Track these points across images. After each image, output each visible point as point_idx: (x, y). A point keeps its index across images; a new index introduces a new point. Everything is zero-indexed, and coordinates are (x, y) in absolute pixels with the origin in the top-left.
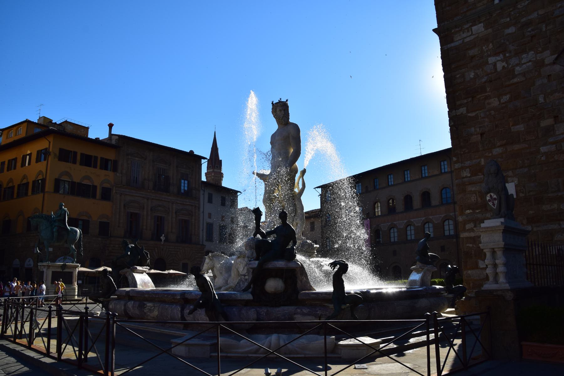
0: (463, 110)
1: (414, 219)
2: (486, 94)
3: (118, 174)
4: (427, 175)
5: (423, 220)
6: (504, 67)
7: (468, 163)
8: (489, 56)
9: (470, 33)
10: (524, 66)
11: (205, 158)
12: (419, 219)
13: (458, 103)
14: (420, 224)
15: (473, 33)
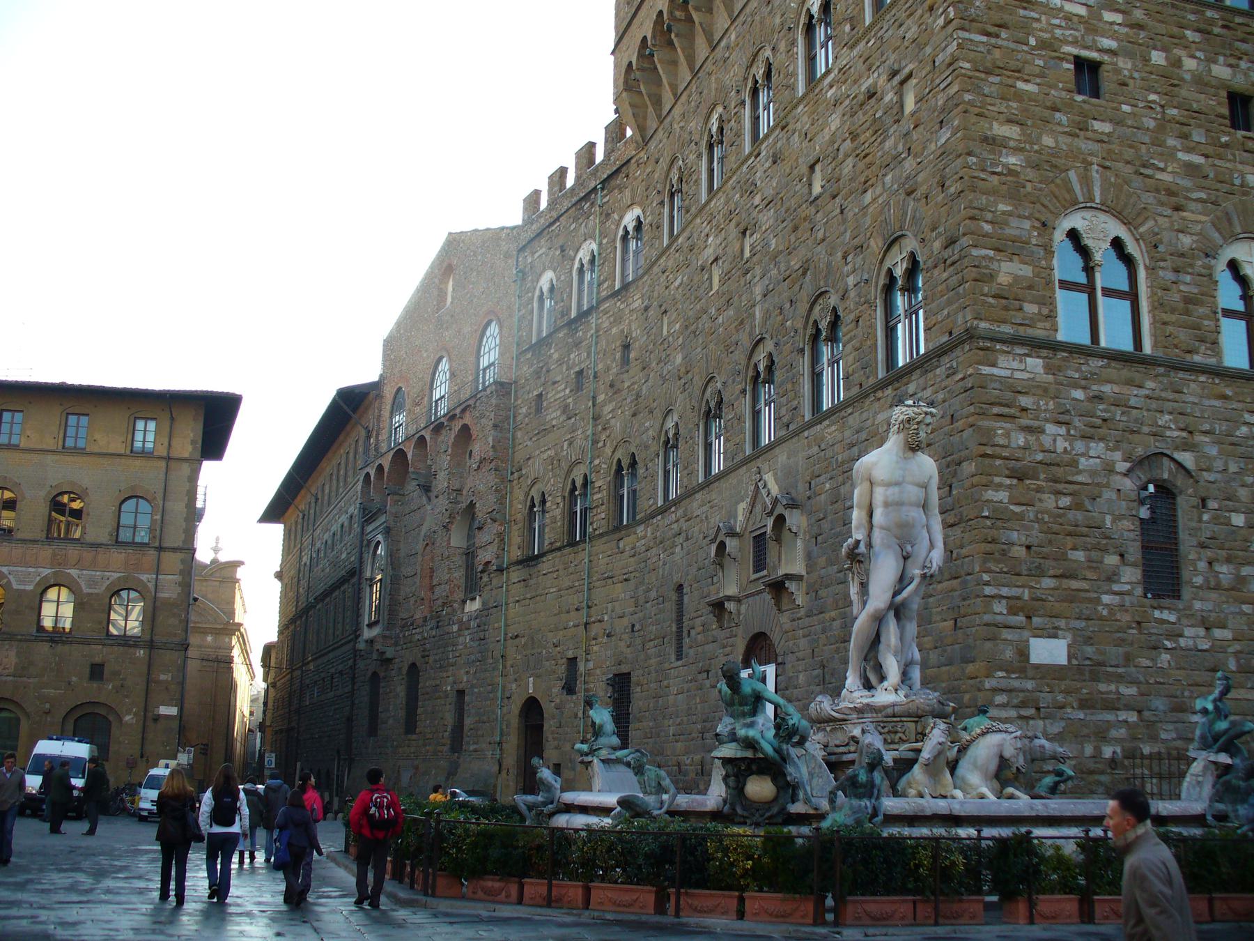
0: (1003, 496)
2: (1039, 483)
4: (81, 444)
6: (1065, 448)
7: (1005, 591)
8: (1047, 420)
10: (1091, 460)
12: (30, 569)
13: (997, 480)
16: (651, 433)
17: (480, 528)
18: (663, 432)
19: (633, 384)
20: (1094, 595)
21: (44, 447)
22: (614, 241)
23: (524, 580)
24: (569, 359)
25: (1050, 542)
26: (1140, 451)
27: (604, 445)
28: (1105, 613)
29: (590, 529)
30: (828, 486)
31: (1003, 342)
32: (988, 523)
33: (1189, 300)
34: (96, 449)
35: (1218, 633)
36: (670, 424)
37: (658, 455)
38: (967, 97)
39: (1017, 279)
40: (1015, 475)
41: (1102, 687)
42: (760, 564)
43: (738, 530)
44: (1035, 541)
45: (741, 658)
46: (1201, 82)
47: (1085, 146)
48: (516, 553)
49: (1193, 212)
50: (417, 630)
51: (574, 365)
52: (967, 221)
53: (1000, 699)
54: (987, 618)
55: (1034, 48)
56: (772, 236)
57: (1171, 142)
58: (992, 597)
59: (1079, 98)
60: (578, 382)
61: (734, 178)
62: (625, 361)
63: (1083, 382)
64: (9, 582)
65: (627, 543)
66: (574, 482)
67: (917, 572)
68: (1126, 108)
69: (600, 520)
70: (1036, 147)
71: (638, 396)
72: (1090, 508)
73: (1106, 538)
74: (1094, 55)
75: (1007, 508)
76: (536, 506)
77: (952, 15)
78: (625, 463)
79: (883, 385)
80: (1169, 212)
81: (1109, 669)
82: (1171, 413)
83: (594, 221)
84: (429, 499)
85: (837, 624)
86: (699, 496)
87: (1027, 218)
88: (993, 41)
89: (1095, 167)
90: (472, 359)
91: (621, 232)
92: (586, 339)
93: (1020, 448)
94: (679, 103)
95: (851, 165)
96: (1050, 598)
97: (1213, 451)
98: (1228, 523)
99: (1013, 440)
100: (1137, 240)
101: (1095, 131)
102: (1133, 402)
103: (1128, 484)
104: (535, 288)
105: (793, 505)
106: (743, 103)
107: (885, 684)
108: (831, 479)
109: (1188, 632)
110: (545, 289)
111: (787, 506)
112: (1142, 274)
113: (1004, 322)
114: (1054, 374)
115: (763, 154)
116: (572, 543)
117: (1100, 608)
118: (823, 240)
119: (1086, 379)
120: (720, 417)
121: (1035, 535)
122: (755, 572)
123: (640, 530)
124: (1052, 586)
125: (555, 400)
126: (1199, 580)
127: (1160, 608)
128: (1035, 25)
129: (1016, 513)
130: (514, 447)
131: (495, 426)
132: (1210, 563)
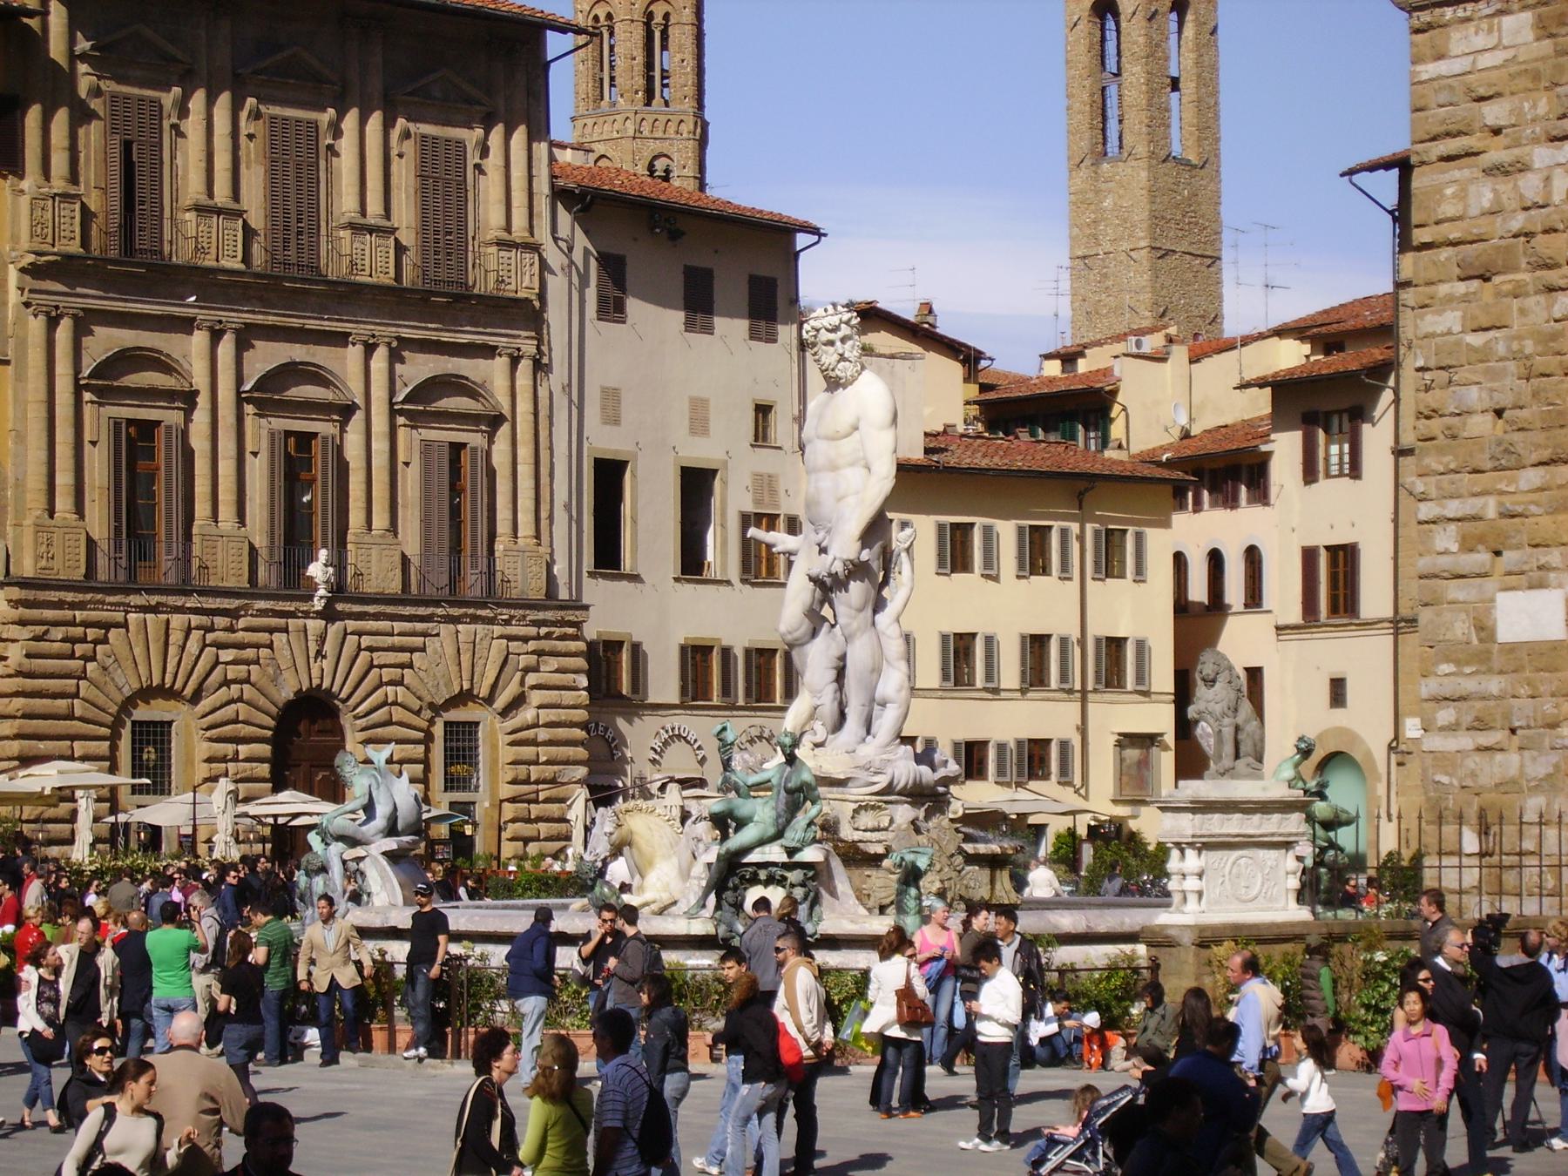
0: (1451, 320)
3: (25, 185)
7: (1453, 508)
8: (1535, 141)
11: (564, 28)
13: (1443, 289)
15: (1505, 42)
25: (1535, 394)
40: (1472, 273)
44: (1505, 400)
53: (1445, 715)
75: (1458, 343)
96: (1533, 509)
99: (1472, 201)
114: (1552, 36)
121: (1510, 387)
124: (1537, 482)
129: (1470, 347)
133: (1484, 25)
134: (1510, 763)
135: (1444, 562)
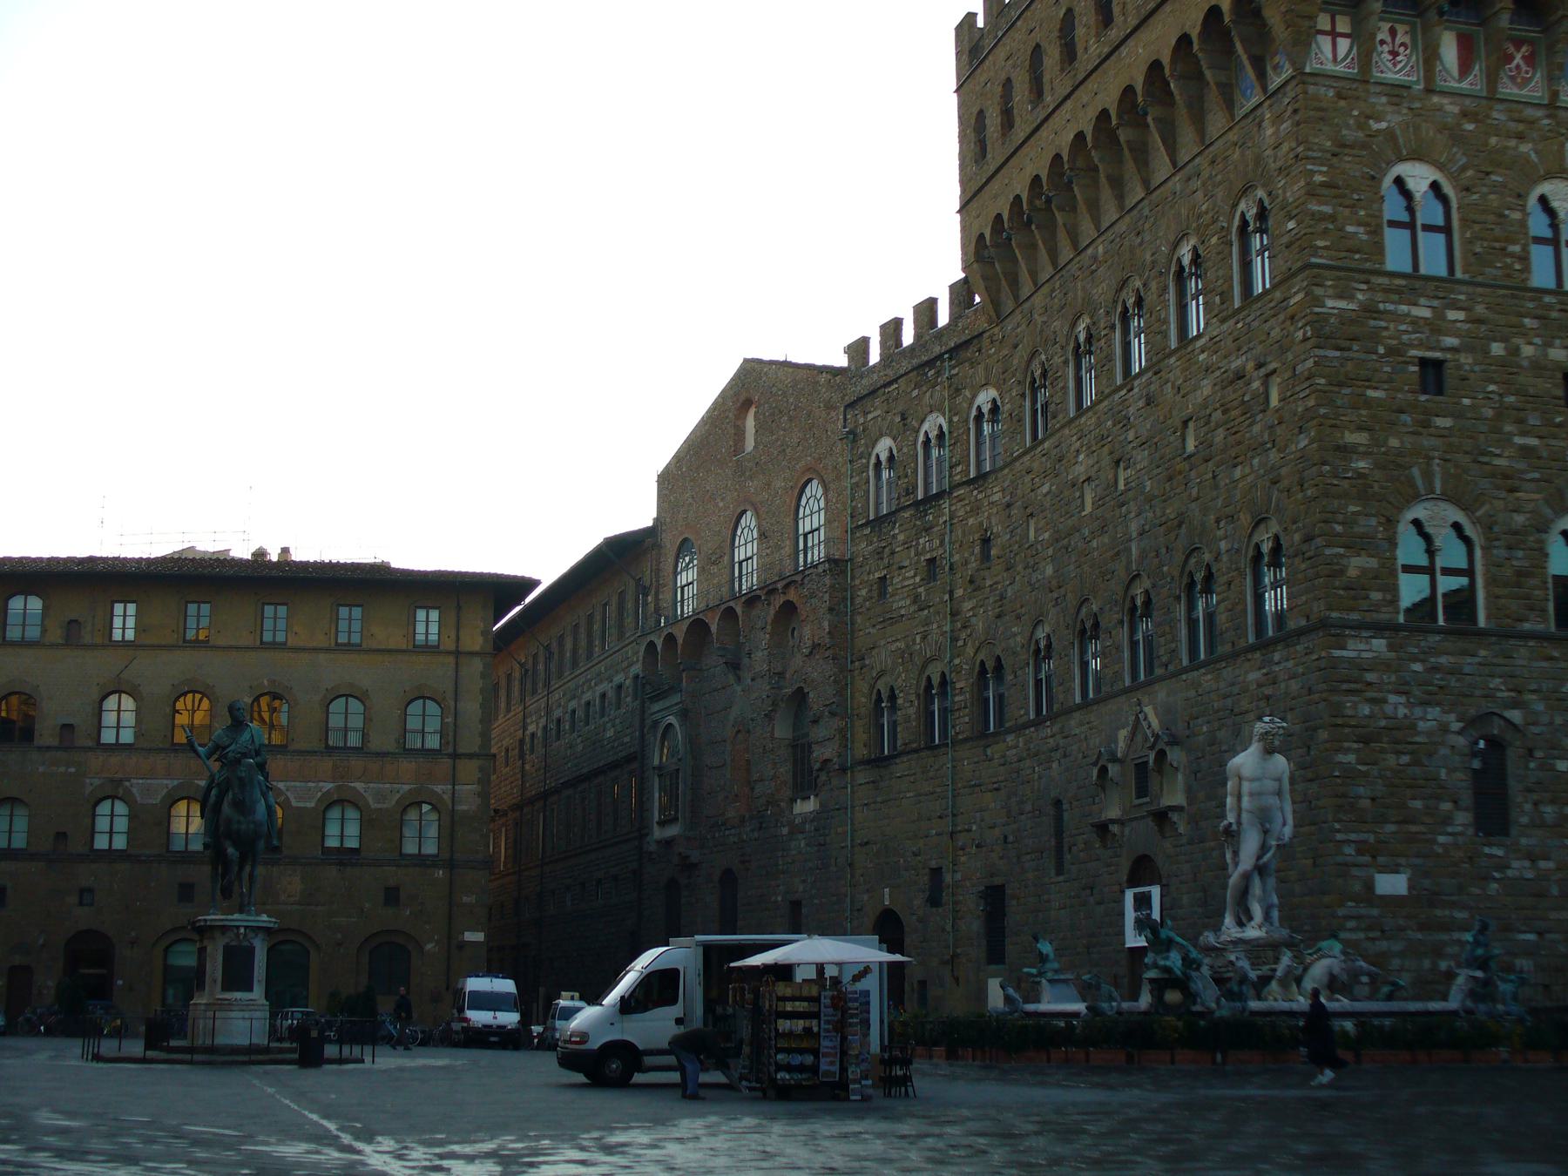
0: (1351, 758)
1: (288, 784)
5: (324, 790)
6: (1405, 715)
7: (1353, 837)
8: (1389, 692)
9: (1367, 647)
10: (1429, 723)
13: (1346, 745)
14: (312, 804)
16: (1018, 639)
17: (815, 722)
18: (1033, 641)
19: (996, 583)
20: (1430, 836)
21: (315, 644)
22: (967, 421)
23: (873, 782)
24: (918, 544)
26: (1472, 712)
27: (965, 644)
28: (1440, 850)
29: (951, 732)
30: (1205, 729)
31: (1351, 628)
32: (1339, 781)
33: (1520, 573)
34: (375, 646)
35: (1543, 864)
36: (1041, 634)
37: (1028, 664)
38: (1322, 411)
39: (1364, 571)
41: (1439, 912)
42: (1142, 791)
43: (1119, 755)
45: (1125, 878)
46: (1538, 367)
47: (1427, 442)
48: (861, 751)
49: (1526, 492)
50: (733, 831)
51: (924, 552)
52: (1322, 525)
53: (1351, 924)
54: (1339, 859)
55: (1382, 356)
56: (1146, 478)
57: (1508, 428)
58: (1343, 842)
59: (1423, 398)
60: (929, 571)
61: (1106, 403)
62: (985, 556)
63: (1422, 656)
64: (287, 798)
65: (995, 750)
66: (929, 679)
67: (1274, 843)
68: (1466, 401)
69: (963, 722)
70: (1383, 449)
71: (1002, 598)
72: (1427, 763)
73: (1444, 788)
74: (1437, 355)
76: (885, 702)
77: (1309, 334)
78: (990, 665)
79: (1252, 649)
80: (1503, 494)
81: (1444, 898)
82: (1501, 677)
83: (941, 392)
84: (739, 679)
85: (1215, 854)
86: (1077, 715)
87: (1374, 516)
88: (1346, 354)
89: (1437, 461)
90: (789, 520)
91: (974, 413)
92: (937, 525)
93: (1366, 716)
94: (1039, 293)
95: (1222, 436)
97: (1540, 707)
98: (1553, 768)
100: (1474, 523)
101: (1437, 427)
102: (1467, 669)
103: (1461, 741)
104: (870, 455)
105: (1174, 741)
106: (1113, 327)
107: (1253, 923)
108: (1208, 722)
109: (1516, 864)
110: (884, 457)
111: (1168, 744)
112: (1478, 553)
113: (1352, 609)
115: (1136, 390)
116: (931, 747)
117: (1435, 847)
118: (1197, 499)
119: (1424, 653)
120: (1097, 638)
122: (1138, 797)
123: (1010, 738)
125: (903, 587)
126: (1524, 820)
127: (1490, 845)
128: (1385, 334)
130: (853, 631)
131: (831, 610)
132: (1536, 804)
133: (1364, 640)
134: (1383, 945)
135: (1348, 858)
